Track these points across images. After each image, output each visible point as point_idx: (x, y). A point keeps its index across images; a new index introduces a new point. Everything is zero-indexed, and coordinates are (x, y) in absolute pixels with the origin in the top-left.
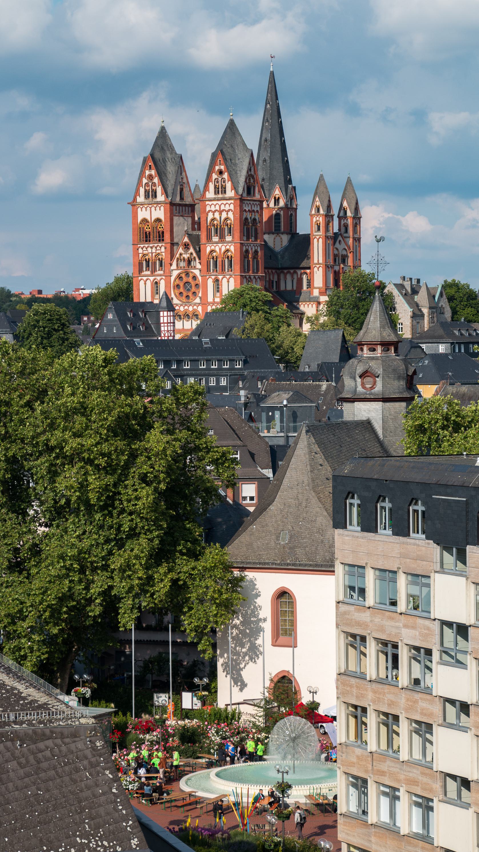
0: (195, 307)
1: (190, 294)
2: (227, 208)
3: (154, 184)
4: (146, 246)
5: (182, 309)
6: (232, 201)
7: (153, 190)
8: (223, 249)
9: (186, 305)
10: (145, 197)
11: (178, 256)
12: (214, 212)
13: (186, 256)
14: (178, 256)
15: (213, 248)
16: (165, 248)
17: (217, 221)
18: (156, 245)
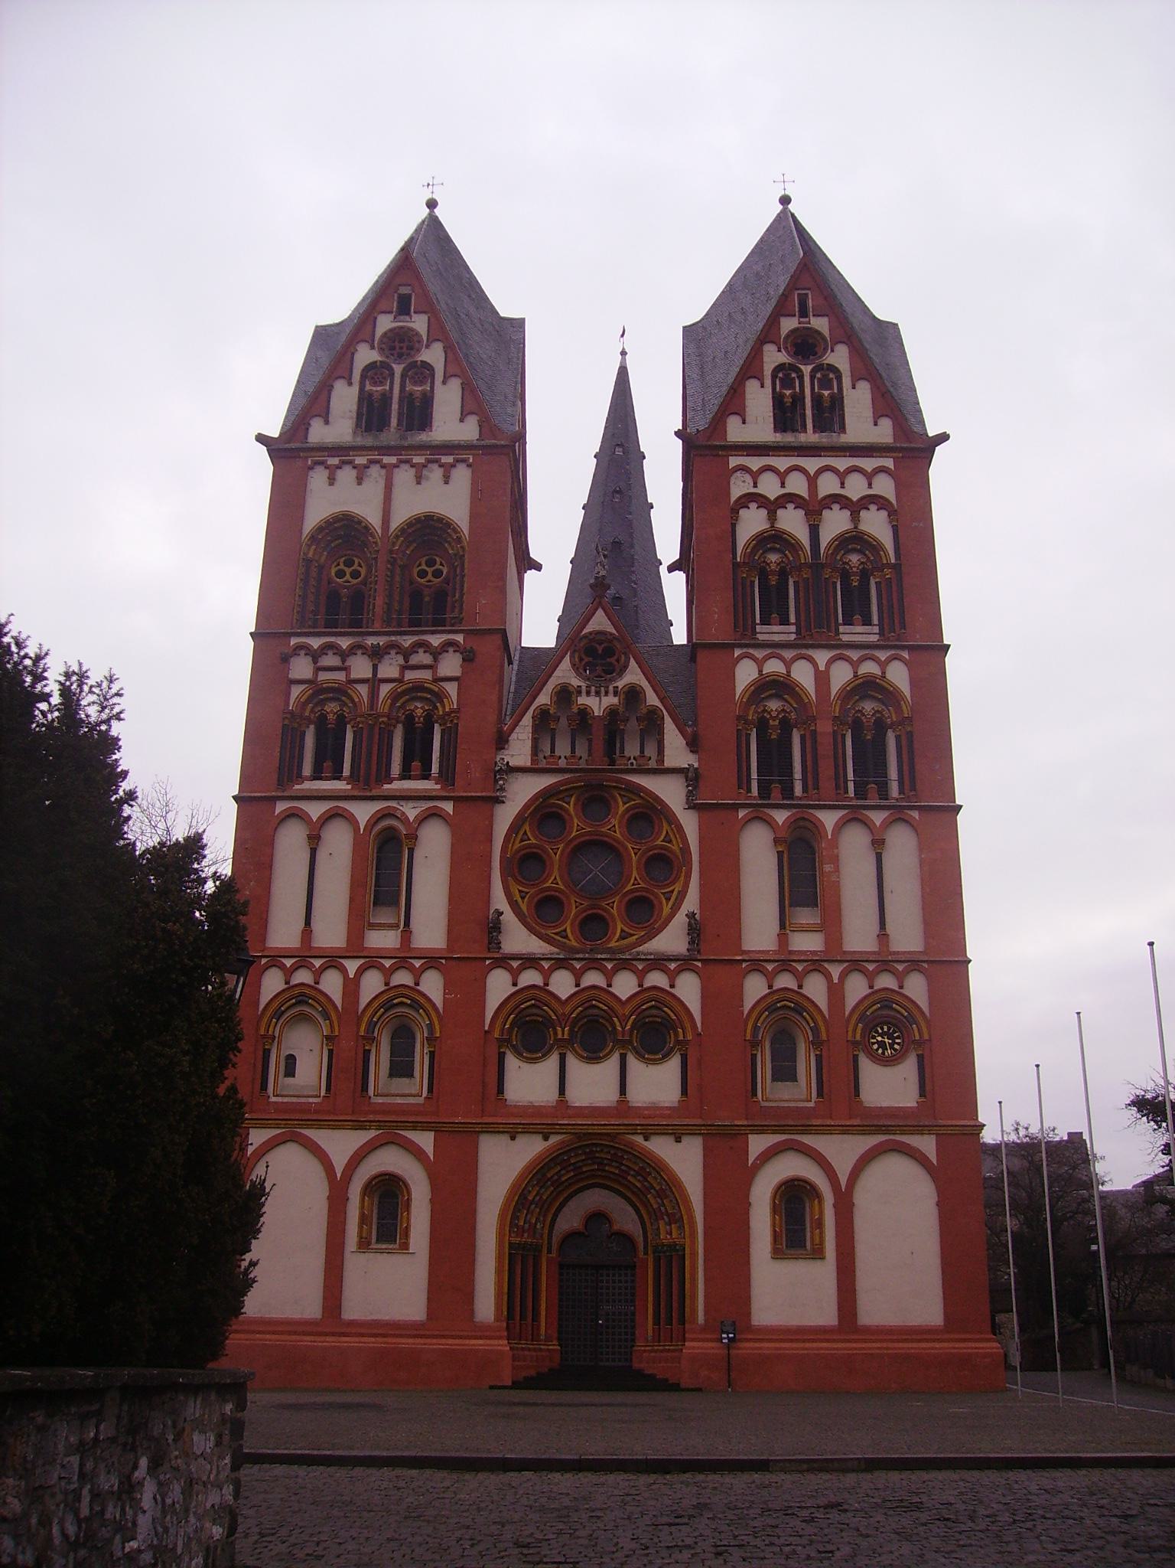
0: (656, 979)
1: (615, 908)
2: (856, 488)
3: (425, 372)
4: (345, 643)
5: (562, 985)
6: (889, 463)
7: (407, 398)
8: (841, 675)
9: (594, 964)
10: (358, 425)
11: (544, 699)
12: (772, 507)
13: (597, 705)
14: (544, 699)
15: (774, 667)
16: (469, 657)
17: (793, 545)
18: (407, 641)
